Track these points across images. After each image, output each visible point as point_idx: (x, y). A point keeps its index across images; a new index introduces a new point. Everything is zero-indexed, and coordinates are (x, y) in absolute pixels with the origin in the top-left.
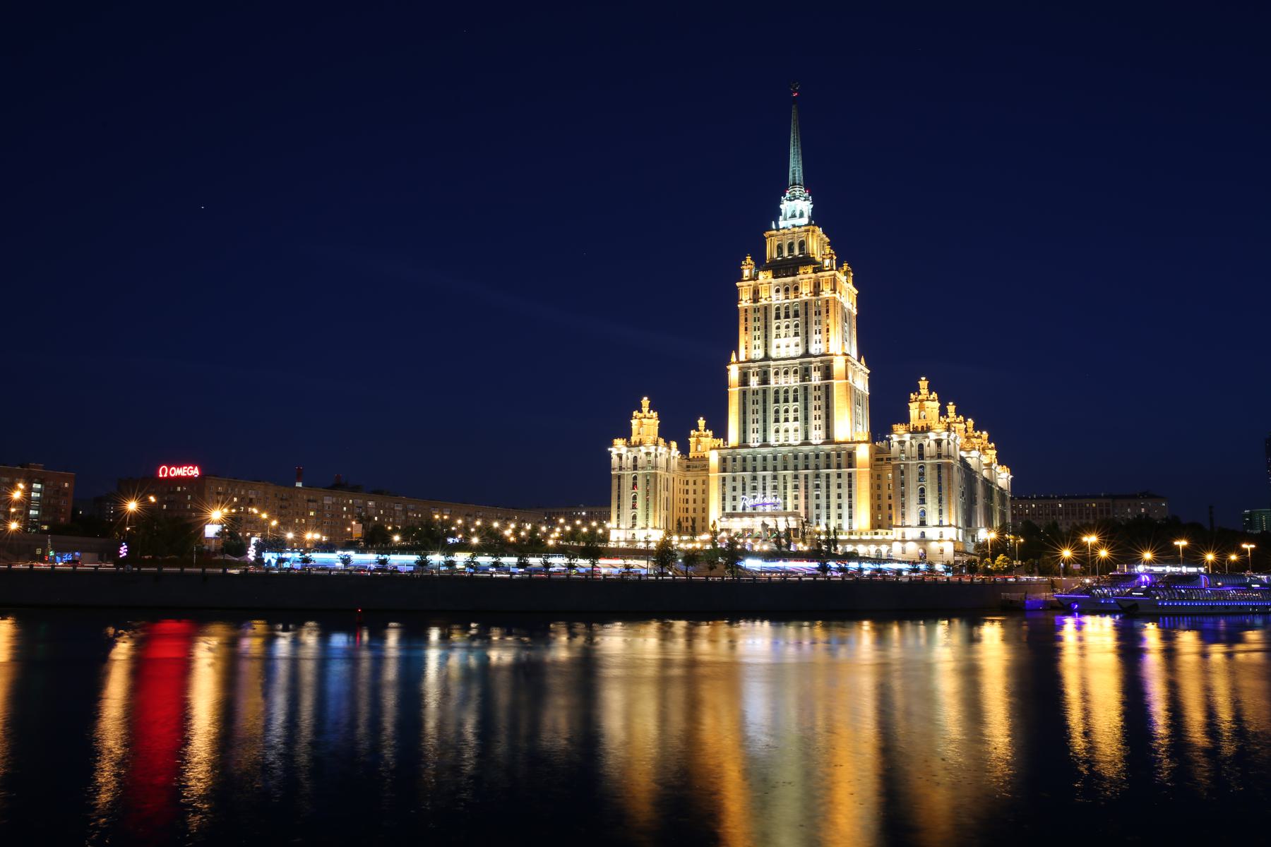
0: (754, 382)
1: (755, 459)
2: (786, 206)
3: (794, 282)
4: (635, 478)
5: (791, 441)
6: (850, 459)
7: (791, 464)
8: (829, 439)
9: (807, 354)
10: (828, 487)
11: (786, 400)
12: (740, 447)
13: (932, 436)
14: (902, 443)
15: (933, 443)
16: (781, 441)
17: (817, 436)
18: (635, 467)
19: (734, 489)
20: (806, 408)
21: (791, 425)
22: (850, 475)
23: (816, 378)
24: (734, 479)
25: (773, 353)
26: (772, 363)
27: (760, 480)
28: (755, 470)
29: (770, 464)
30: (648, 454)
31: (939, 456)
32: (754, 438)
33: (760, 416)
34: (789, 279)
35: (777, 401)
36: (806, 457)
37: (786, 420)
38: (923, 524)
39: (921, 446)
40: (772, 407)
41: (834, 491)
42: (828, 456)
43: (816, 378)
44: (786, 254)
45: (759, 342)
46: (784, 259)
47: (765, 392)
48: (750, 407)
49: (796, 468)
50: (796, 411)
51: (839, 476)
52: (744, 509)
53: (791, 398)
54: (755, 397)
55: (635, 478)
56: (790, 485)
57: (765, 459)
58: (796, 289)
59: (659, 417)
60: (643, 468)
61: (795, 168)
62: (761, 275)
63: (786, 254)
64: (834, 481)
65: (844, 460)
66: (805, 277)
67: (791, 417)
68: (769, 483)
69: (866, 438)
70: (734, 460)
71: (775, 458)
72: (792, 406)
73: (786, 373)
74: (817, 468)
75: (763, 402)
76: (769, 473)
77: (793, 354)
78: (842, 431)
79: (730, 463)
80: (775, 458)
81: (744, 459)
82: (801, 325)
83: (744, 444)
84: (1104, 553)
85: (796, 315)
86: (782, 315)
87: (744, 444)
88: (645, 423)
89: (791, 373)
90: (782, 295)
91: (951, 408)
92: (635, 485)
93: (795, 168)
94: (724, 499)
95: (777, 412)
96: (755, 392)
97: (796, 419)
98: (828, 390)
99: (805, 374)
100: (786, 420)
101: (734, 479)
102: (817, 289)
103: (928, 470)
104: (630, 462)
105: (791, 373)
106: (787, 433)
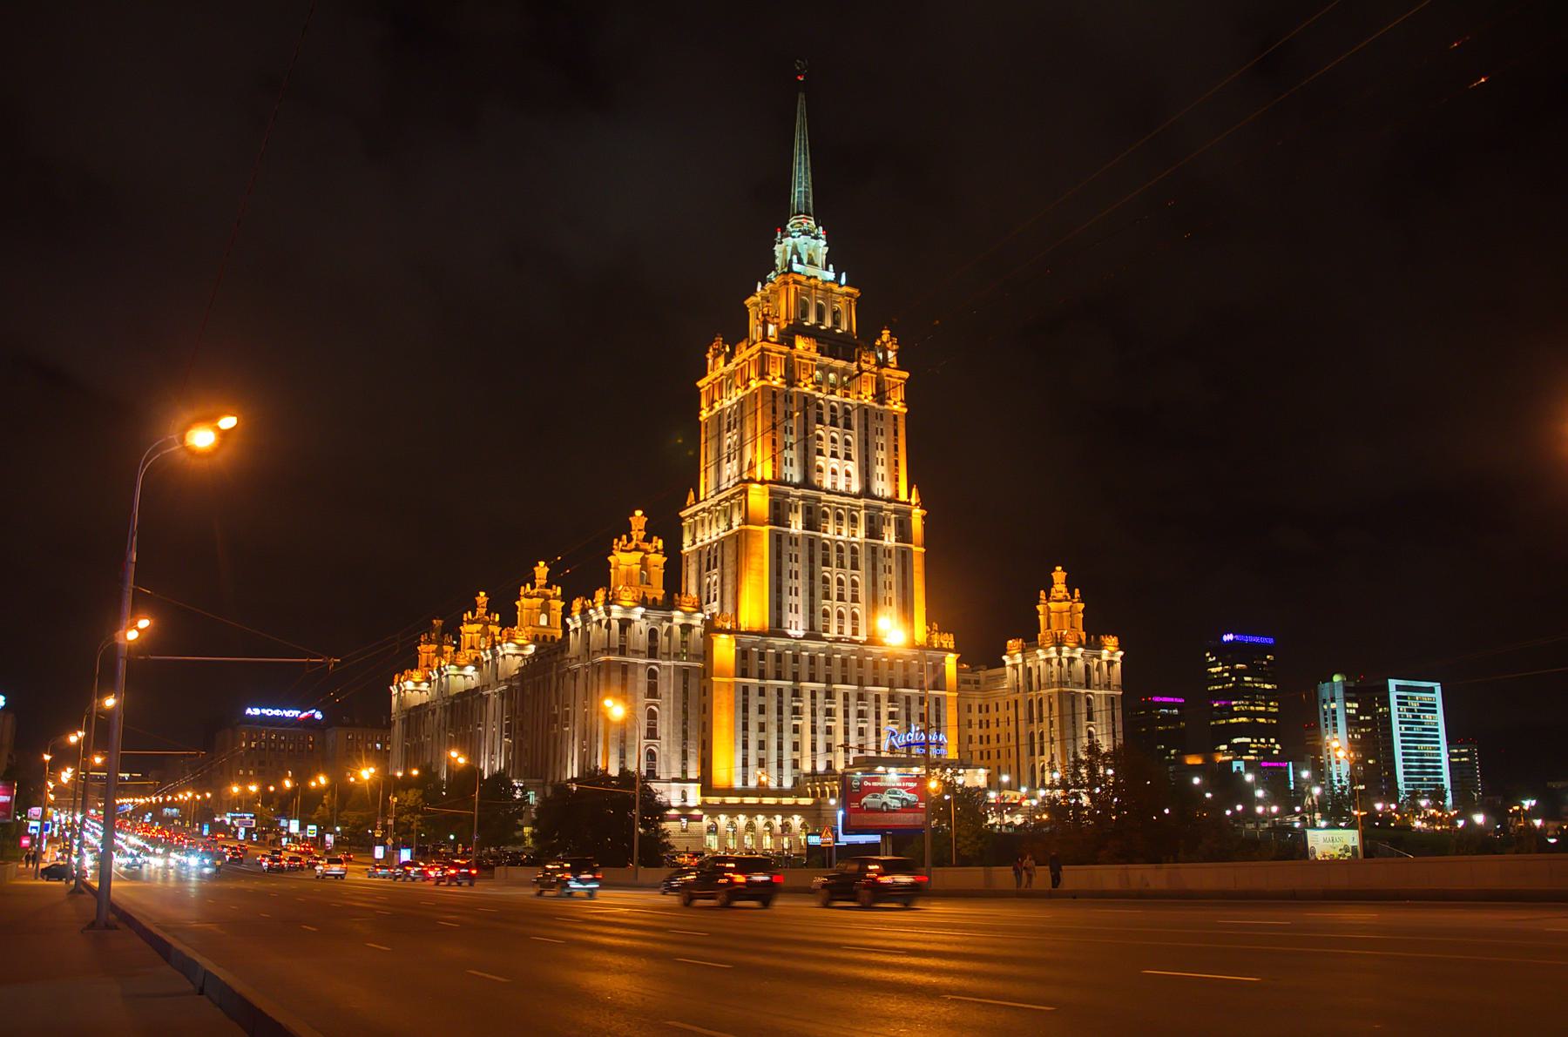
1: (796, 658)
4: (652, 674)
7: (854, 672)
9: (866, 492)
10: (908, 718)
13: (1105, 654)
14: (1071, 660)
15: (1105, 665)
18: (652, 652)
20: (874, 583)
22: (937, 701)
23: (889, 539)
24: (762, 692)
25: (816, 478)
26: (824, 497)
31: (1108, 686)
32: (796, 625)
33: (801, 583)
39: (1087, 667)
50: (854, 584)
52: (892, 748)
54: (793, 550)
55: (652, 674)
56: (853, 711)
57: (812, 659)
60: (677, 656)
61: (801, 188)
62: (800, 343)
69: (952, 646)
70: (762, 656)
76: (819, 686)
77: (841, 486)
79: (755, 663)
80: (828, 661)
84: (253, 788)
86: (827, 419)
87: (777, 628)
93: (801, 188)
94: (745, 727)
96: (794, 540)
98: (905, 555)
101: (762, 692)
103: (1096, 706)
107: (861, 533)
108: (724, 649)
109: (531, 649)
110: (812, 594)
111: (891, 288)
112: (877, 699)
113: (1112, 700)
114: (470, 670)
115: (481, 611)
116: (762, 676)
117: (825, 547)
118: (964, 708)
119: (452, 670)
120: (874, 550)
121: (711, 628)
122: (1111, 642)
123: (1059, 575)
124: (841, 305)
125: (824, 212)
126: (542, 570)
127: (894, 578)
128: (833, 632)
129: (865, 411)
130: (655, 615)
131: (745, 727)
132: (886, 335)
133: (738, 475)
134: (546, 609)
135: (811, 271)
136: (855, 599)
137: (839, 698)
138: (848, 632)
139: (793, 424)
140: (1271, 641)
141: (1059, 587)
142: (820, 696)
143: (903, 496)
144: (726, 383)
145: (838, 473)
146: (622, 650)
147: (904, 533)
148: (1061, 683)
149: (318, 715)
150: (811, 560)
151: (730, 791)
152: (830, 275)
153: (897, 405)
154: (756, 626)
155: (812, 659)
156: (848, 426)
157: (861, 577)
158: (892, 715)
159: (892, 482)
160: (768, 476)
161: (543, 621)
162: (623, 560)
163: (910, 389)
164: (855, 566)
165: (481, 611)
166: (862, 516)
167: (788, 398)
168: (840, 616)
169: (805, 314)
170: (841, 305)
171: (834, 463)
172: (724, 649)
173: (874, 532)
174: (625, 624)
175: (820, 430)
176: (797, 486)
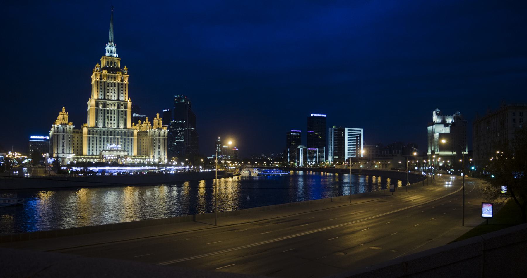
0: (101, 107)
1: (100, 131)
2: (108, 48)
4: (64, 136)
5: (113, 127)
6: (132, 134)
8: (125, 128)
9: (118, 100)
11: (111, 114)
13: (163, 130)
14: (155, 132)
16: (109, 126)
17: (122, 126)
18: (64, 132)
19: (93, 141)
21: (113, 122)
22: (132, 139)
23: (122, 108)
24: (93, 138)
27: (102, 139)
28: (100, 135)
29: (106, 134)
30: (70, 128)
32: (101, 125)
33: (102, 118)
34: (113, 75)
35: (108, 113)
36: (118, 132)
37: (111, 120)
38: (159, 154)
40: (106, 115)
41: (127, 143)
42: (125, 133)
43: (122, 108)
45: (102, 93)
46: (109, 67)
47: (104, 110)
48: (99, 115)
49: (114, 136)
51: (128, 139)
53: (113, 113)
55: (64, 136)
57: (104, 132)
58: (115, 78)
59: (68, 114)
61: (111, 36)
62: (104, 71)
63: (109, 65)
64: (126, 140)
65: (130, 134)
66: (119, 75)
67: (113, 119)
68: (105, 140)
70: (93, 131)
71: (107, 132)
72: (113, 116)
73: (111, 105)
74: (114, 136)
75: (102, 113)
76: (105, 136)
78: (129, 126)
79: (91, 133)
80: (107, 132)
83: (96, 126)
85: (115, 87)
87: (96, 126)
88: (63, 116)
89: (113, 105)
90: (110, 79)
92: (63, 139)
93: (111, 36)
94: (89, 144)
95: (108, 117)
96: (101, 110)
97: (114, 120)
98: (126, 113)
99: (118, 107)
100: (111, 120)
101: (93, 138)
103: (161, 140)
104: (62, 130)
105: (113, 105)
106: (112, 125)
107: (116, 107)
110: (104, 119)
112: (118, 139)
113: (164, 139)
116: (93, 135)
117: (108, 111)
118: (139, 140)
120: (118, 111)
125: (116, 42)
128: (109, 126)
129: (119, 84)
130: (63, 126)
131: (89, 144)
136: (114, 120)
137: (110, 139)
140: (325, 116)
141: (158, 117)
143: (127, 100)
146: (58, 132)
148: (152, 136)
150: (104, 113)
151: (86, 155)
153: (126, 82)
155: (104, 132)
157: (115, 116)
158: (121, 142)
159: (124, 97)
160: (96, 98)
164: (114, 114)
166: (116, 104)
167: (101, 82)
168: (111, 123)
171: (111, 94)
172: (85, 130)
174: (58, 128)
175: (108, 88)
176: (101, 99)
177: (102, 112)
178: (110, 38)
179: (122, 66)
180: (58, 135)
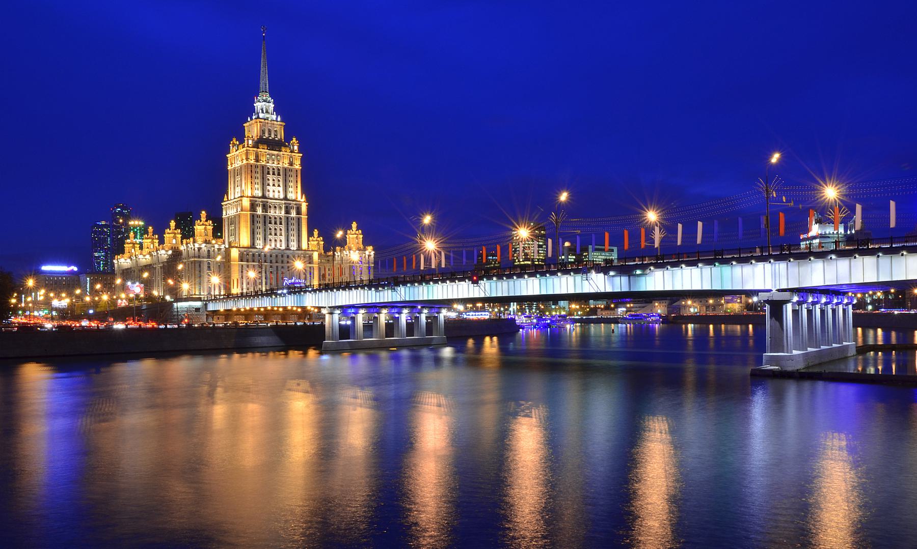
0: (259, 211)
2: (258, 105)
3: (278, 155)
5: (278, 246)
8: (299, 248)
9: (286, 198)
11: (275, 223)
12: (251, 248)
13: (367, 253)
17: (294, 246)
21: (278, 238)
23: (293, 214)
32: (259, 244)
33: (261, 231)
43: (293, 214)
44: (267, 135)
46: (267, 139)
61: (264, 81)
63: (267, 135)
72: (278, 227)
76: (268, 264)
77: (276, 197)
78: (304, 246)
81: (253, 255)
82: (262, 177)
83: (253, 246)
87: (253, 246)
91: (316, 232)
93: (264, 81)
96: (258, 216)
98: (299, 220)
102: (291, 164)
107: (283, 212)
108: (235, 253)
109: (170, 252)
111: (297, 123)
114: (148, 257)
115: (150, 234)
116: (248, 261)
119: (141, 257)
121: (230, 246)
122: (370, 248)
123: (354, 225)
124: (278, 128)
126: (173, 224)
127: (295, 227)
132: (294, 139)
133: (240, 194)
134: (175, 238)
135: (267, 115)
136: (281, 235)
138: (278, 246)
139: (259, 175)
141: (354, 229)
142: (268, 268)
143: (299, 199)
144: (237, 158)
145: (275, 191)
146: (199, 257)
147: (299, 212)
149: (75, 269)
152: (274, 117)
153: (297, 166)
154: (246, 245)
156: (279, 175)
157: (283, 227)
159: (296, 193)
161: (174, 241)
162: (199, 228)
163: (302, 159)
164: (281, 224)
165: (150, 234)
169: (263, 132)
170: (278, 128)
172: (235, 253)
173: (287, 212)
174: (199, 249)
177: (261, 220)
178: (262, 85)
179: (288, 138)
180: (200, 262)
